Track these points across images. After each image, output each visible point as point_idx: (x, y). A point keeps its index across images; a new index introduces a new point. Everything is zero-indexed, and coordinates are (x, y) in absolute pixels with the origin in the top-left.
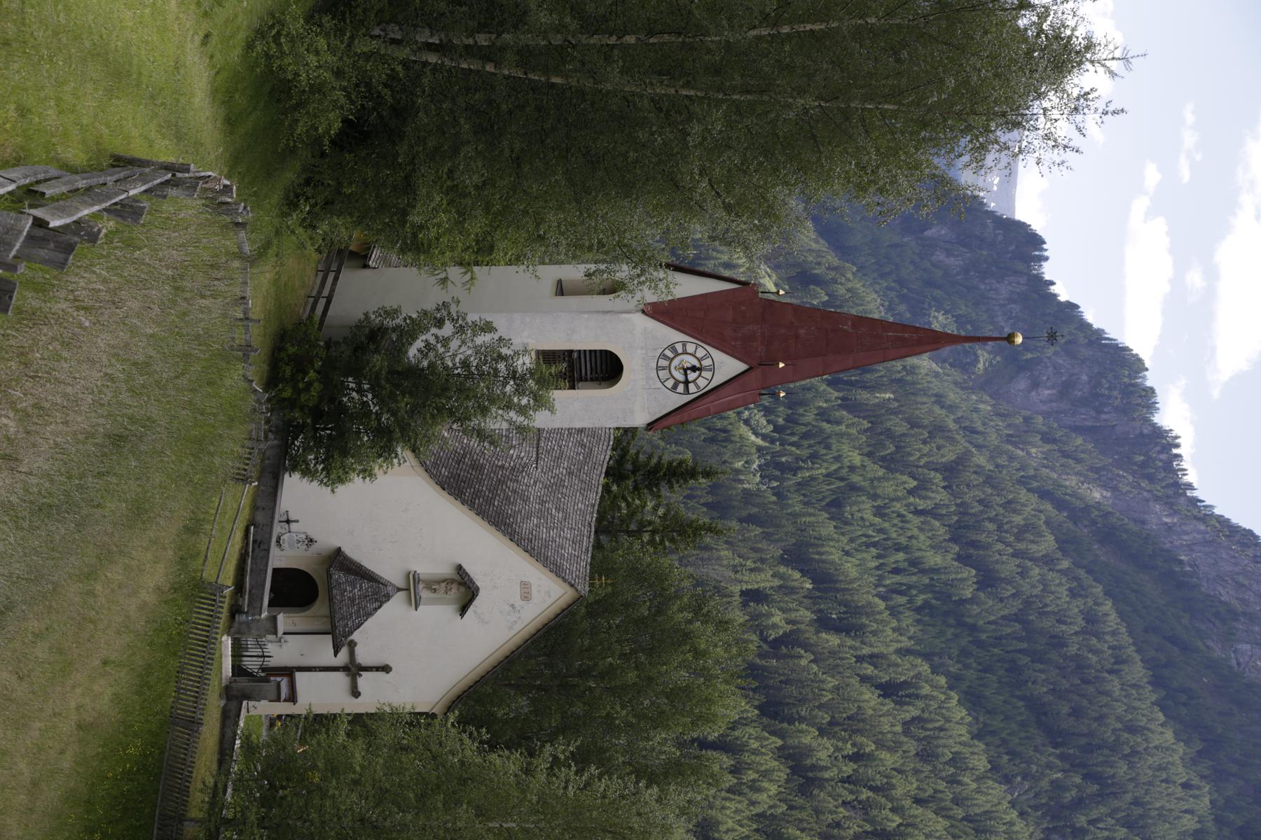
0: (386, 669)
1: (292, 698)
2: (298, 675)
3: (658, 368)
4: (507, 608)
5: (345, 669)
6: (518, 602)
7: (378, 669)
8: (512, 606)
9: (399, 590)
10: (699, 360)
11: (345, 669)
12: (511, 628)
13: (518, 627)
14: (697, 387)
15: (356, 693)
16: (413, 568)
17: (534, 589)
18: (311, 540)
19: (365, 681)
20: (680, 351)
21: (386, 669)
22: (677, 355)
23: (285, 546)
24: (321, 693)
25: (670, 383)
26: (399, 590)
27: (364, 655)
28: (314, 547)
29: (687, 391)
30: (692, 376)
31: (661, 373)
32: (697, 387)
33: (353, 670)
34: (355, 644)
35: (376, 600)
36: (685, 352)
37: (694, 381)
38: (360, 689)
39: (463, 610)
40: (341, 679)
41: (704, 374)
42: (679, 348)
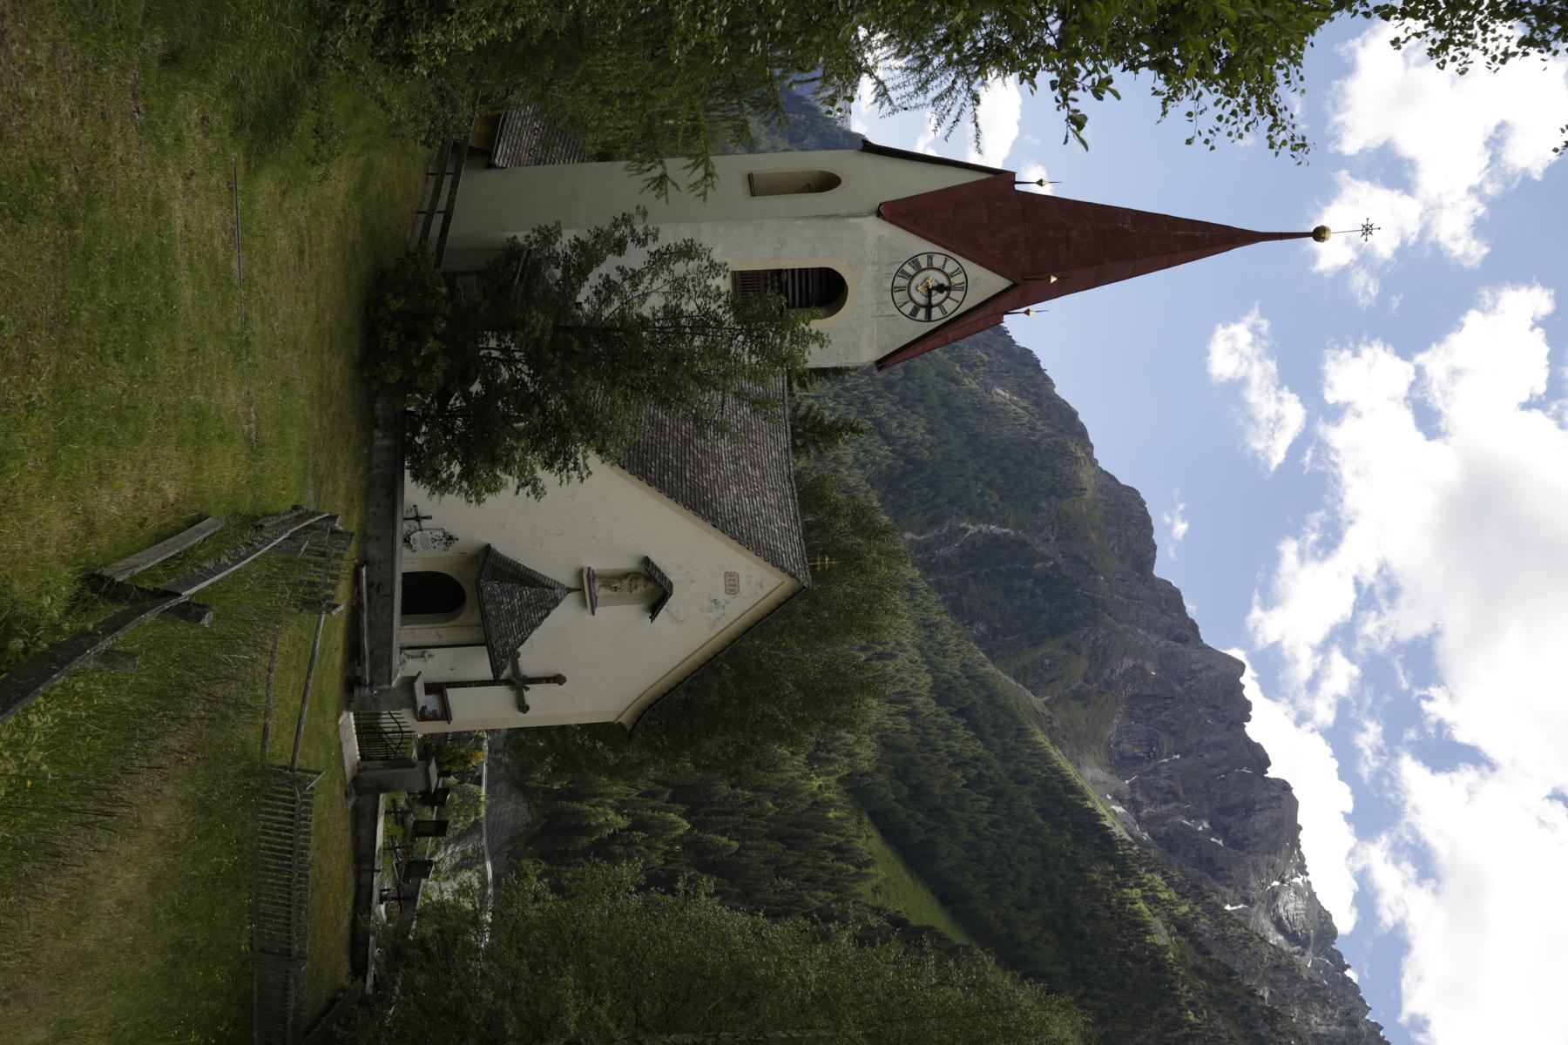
0: (558, 679)
2: (450, 692)
3: (894, 289)
4: (708, 604)
5: (507, 682)
6: (722, 597)
8: (715, 601)
9: (570, 590)
10: (948, 277)
12: (713, 626)
13: (720, 626)
14: (943, 311)
15: (523, 707)
16: (586, 564)
17: (742, 581)
18: (451, 538)
19: (533, 694)
20: (924, 265)
21: (558, 679)
22: (920, 270)
23: (418, 546)
25: (908, 308)
26: (570, 590)
28: (455, 547)
29: (928, 318)
30: (937, 297)
31: (897, 296)
32: (943, 311)
33: (519, 683)
35: (542, 608)
36: (930, 267)
37: (939, 305)
40: (503, 694)
41: (953, 294)
42: (923, 262)
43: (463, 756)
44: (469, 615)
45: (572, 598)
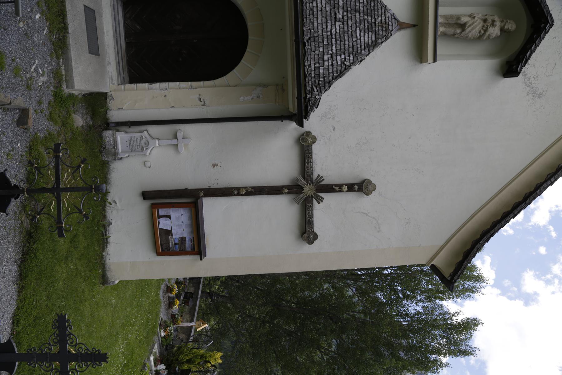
0: (362, 187)
1: (197, 247)
2: (211, 208)
5: (294, 189)
7: (351, 188)
11: (294, 189)
19: (325, 211)
21: (362, 187)
24: (248, 240)
26: (402, 26)
27: (325, 166)
33: (306, 189)
34: (314, 140)
38: (317, 228)
39: (511, 68)
40: (284, 209)
43: (202, 356)
44: (249, 69)
45: (398, 43)
